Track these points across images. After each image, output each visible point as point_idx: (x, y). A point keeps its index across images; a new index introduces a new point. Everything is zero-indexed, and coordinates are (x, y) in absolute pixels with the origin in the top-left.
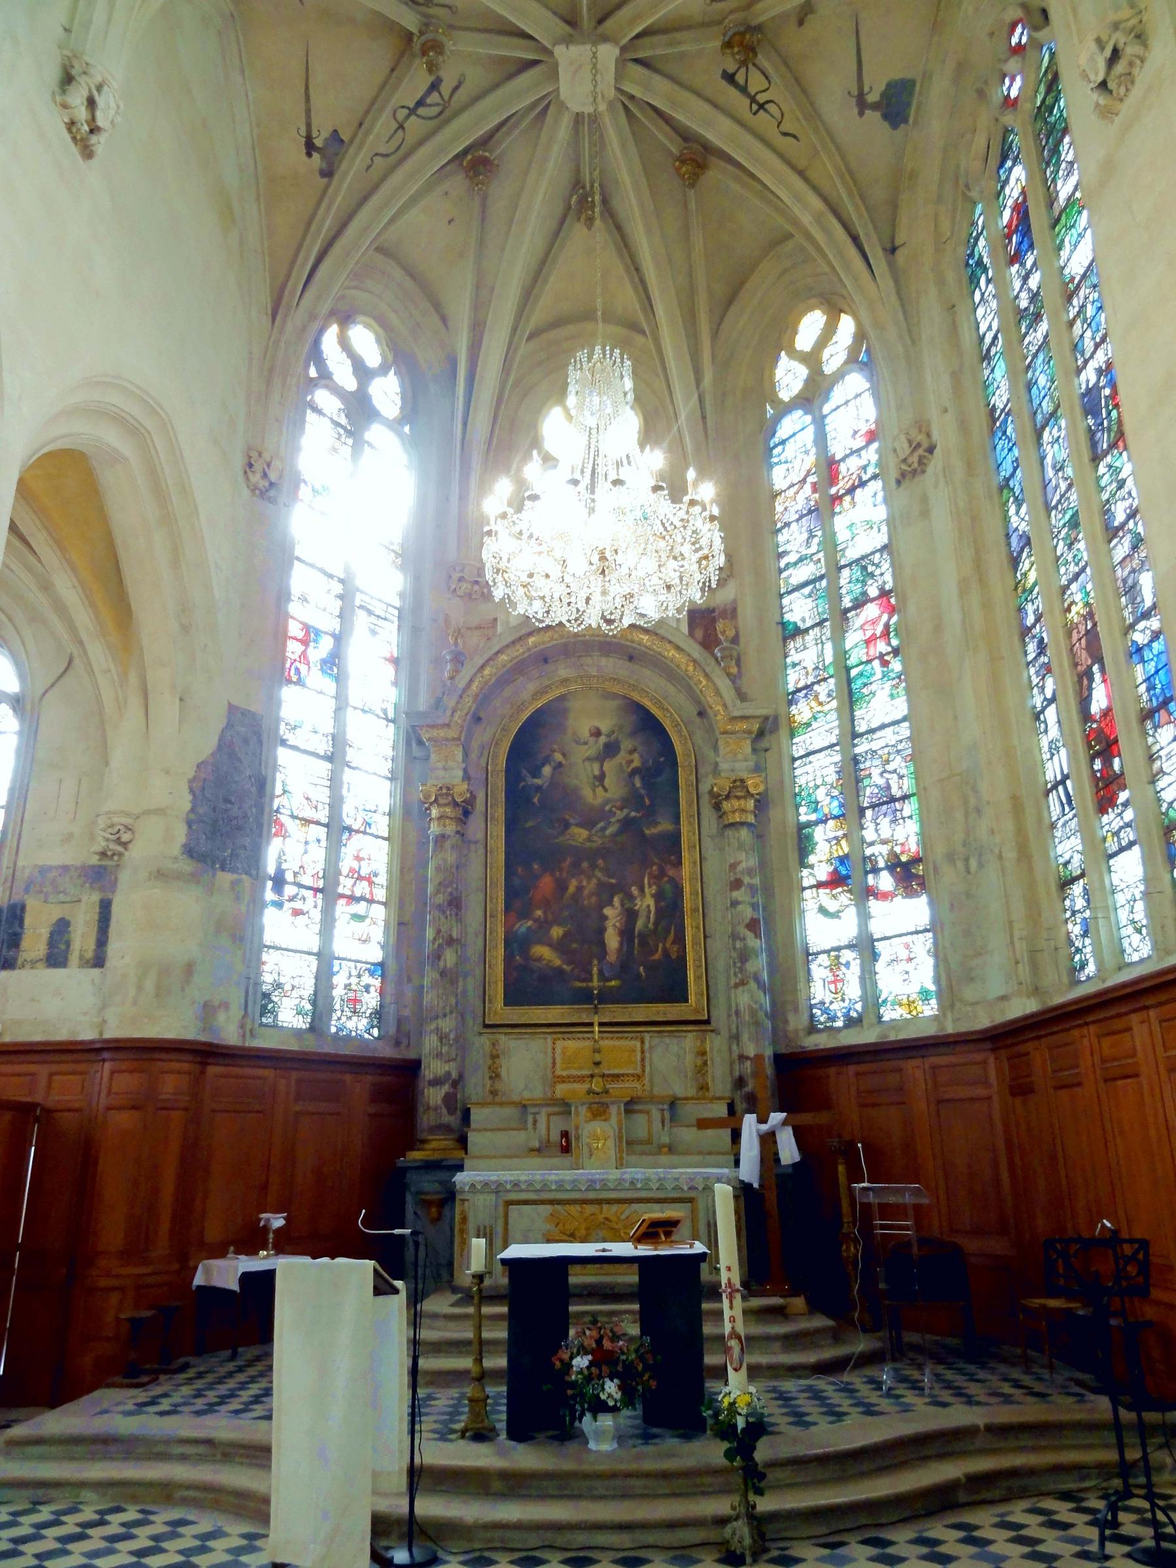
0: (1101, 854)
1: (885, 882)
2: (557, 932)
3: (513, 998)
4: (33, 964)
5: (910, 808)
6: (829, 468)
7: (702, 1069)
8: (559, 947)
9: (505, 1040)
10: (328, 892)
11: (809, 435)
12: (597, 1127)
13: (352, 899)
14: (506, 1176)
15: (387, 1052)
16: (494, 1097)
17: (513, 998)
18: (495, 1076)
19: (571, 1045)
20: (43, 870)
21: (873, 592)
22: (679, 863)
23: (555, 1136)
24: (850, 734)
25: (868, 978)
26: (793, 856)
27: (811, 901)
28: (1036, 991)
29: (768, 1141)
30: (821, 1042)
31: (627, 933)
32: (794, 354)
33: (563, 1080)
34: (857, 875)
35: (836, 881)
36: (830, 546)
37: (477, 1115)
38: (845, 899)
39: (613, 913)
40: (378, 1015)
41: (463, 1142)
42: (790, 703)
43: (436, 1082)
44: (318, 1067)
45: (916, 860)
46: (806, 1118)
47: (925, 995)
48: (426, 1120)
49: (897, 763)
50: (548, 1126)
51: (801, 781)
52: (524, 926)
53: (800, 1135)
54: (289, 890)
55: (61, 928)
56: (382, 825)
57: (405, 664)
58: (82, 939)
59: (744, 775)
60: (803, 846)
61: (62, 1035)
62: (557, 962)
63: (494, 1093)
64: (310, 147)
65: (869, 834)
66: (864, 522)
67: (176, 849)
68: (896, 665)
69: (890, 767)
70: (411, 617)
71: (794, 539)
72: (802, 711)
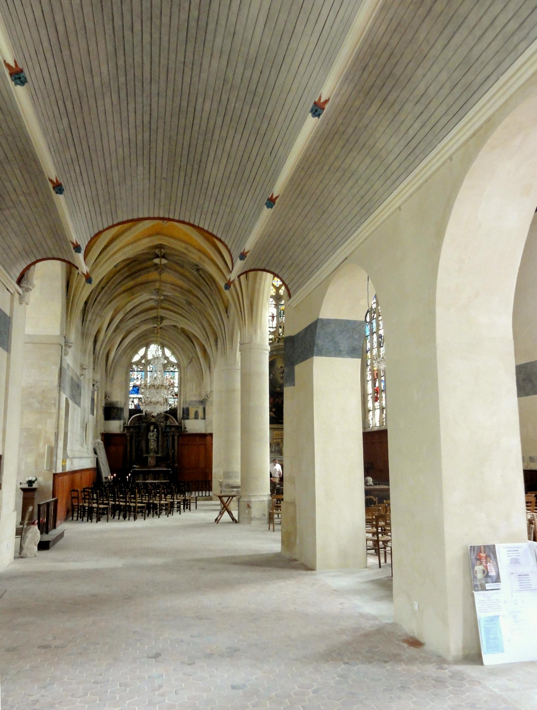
0: (374, 409)
4: (192, 419)
19: (276, 432)
20: (192, 401)
33: (275, 439)
55: (196, 413)
58: (201, 414)
61: (199, 432)
62: (274, 416)
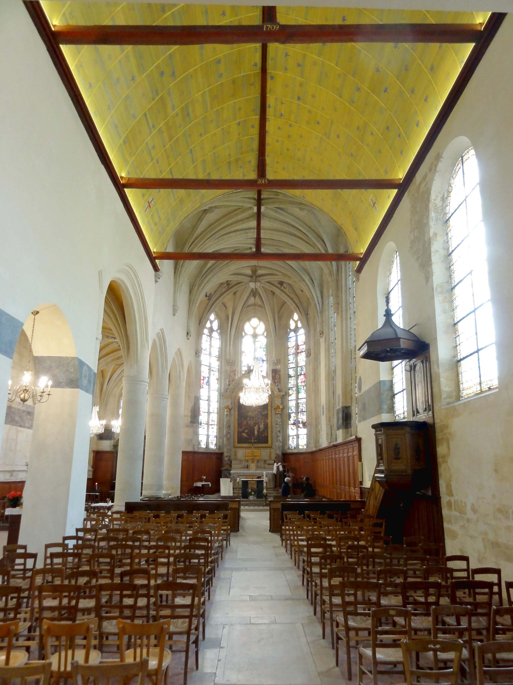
1: (301, 425)
2: (246, 431)
3: (239, 442)
5: (305, 413)
6: (297, 347)
7: (270, 455)
8: (247, 433)
9: (238, 450)
10: (208, 424)
11: (294, 338)
12: (252, 464)
13: (212, 425)
14: (239, 472)
15: (217, 451)
16: (236, 459)
17: (239, 442)
18: (236, 455)
21: (303, 373)
22: (268, 419)
23: (246, 465)
24: (297, 398)
25: (298, 441)
26: (288, 419)
27: (290, 427)
28: (316, 447)
29: (278, 467)
30: (289, 451)
31: (258, 431)
32: (293, 320)
33: (247, 456)
34: (297, 424)
35: (294, 424)
36: (297, 362)
37: (233, 462)
38: (295, 427)
39: (256, 428)
40: (216, 445)
41: (231, 466)
42: (289, 390)
43: (227, 457)
44: (208, 454)
45: (305, 423)
46: (284, 464)
47: (305, 445)
48: (224, 463)
49: (304, 405)
50: (245, 464)
51: (290, 405)
52: (241, 430)
53: (284, 467)
54: (202, 425)
56: (216, 411)
57: (219, 380)
59: (279, 404)
60: (290, 417)
63: (236, 458)
64: (206, 296)
65: (299, 417)
66: (302, 359)
67: (189, 421)
68: (305, 388)
69: (303, 407)
70: (220, 371)
71: (291, 358)
72: (291, 392)
